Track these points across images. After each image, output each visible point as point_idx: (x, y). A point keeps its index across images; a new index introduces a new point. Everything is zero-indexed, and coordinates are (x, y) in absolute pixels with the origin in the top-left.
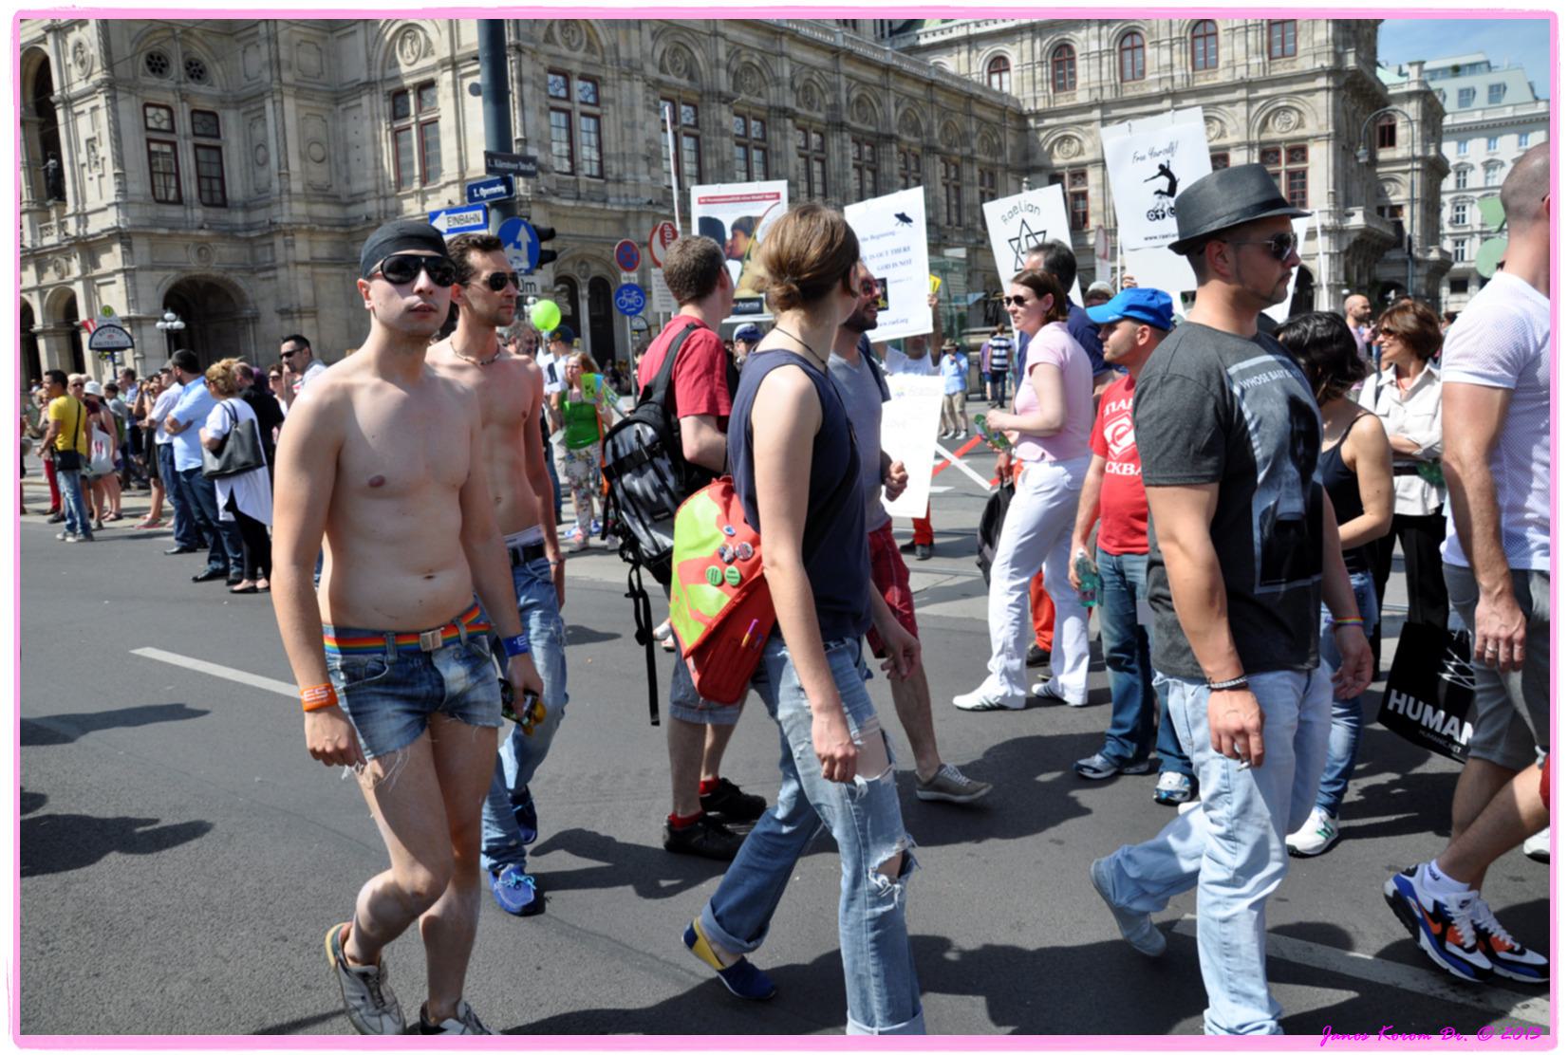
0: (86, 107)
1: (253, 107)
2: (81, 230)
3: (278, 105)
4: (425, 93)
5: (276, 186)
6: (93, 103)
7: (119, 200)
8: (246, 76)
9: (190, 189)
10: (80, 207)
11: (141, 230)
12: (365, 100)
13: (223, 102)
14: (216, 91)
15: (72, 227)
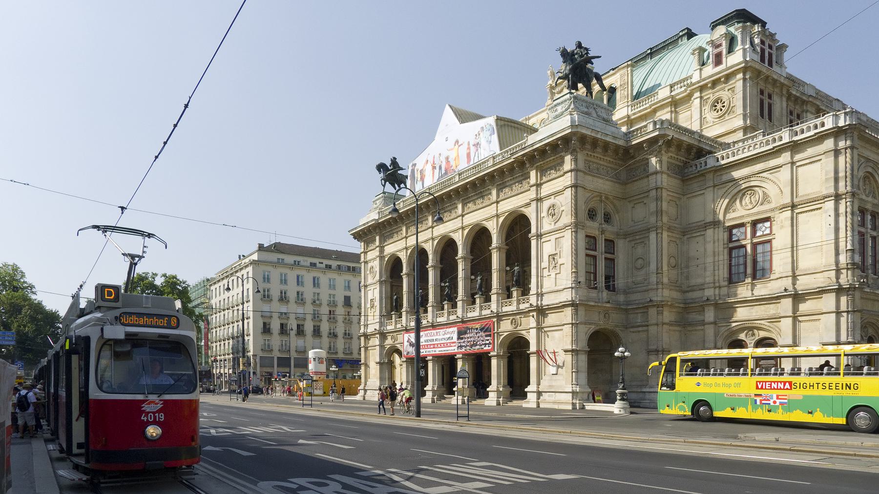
0: (553, 238)
1: (637, 237)
2: (539, 302)
3: (659, 235)
4: (759, 226)
5: (653, 279)
6: (557, 236)
7: (573, 285)
8: (632, 221)
9: (601, 279)
10: (539, 292)
11: (584, 303)
12: (710, 232)
13: (618, 235)
14: (615, 229)
15: (533, 300)
